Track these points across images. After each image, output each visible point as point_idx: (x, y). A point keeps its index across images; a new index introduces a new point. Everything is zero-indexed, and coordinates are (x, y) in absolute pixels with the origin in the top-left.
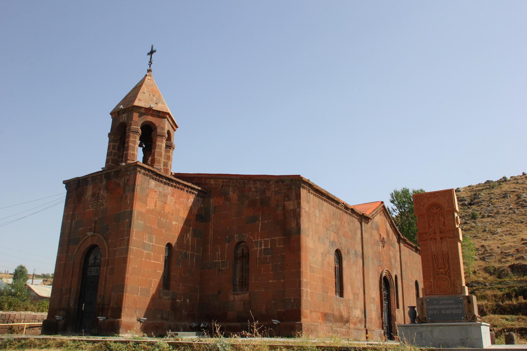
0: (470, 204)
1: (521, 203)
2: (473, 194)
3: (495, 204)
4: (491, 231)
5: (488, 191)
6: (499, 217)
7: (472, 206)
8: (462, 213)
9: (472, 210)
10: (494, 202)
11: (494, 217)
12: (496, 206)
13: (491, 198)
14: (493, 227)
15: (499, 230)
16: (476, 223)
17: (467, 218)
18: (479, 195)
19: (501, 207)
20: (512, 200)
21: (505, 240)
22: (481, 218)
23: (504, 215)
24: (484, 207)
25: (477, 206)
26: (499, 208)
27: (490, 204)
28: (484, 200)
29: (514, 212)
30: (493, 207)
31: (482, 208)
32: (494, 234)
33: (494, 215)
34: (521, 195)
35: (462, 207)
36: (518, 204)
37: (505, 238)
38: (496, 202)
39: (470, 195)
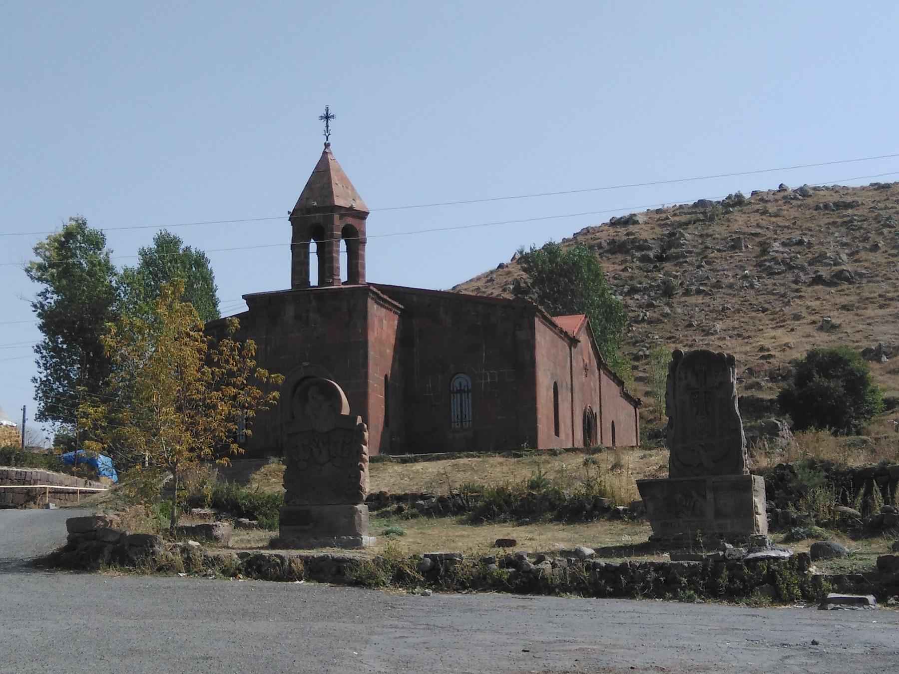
0: (660, 258)
1: (768, 264)
2: (666, 232)
3: (714, 262)
4: (702, 327)
5: (699, 228)
6: (720, 296)
7: (665, 264)
8: (643, 279)
9: (664, 275)
10: (712, 258)
11: (710, 295)
12: (715, 267)
13: (707, 248)
14: (707, 317)
15: (718, 326)
16: (673, 307)
17: (652, 294)
18: (679, 239)
19: (726, 273)
20: (749, 255)
21: (729, 349)
22: (681, 296)
23: (730, 291)
24: (691, 268)
25: (676, 265)
26: (722, 272)
27: (703, 263)
28: (690, 252)
29: (752, 286)
30: (710, 270)
31: (685, 271)
32: (708, 334)
33: (711, 290)
34: (769, 245)
35: (642, 265)
36: (760, 266)
37: (729, 343)
38: (716, 258)
39: (660, 237)
